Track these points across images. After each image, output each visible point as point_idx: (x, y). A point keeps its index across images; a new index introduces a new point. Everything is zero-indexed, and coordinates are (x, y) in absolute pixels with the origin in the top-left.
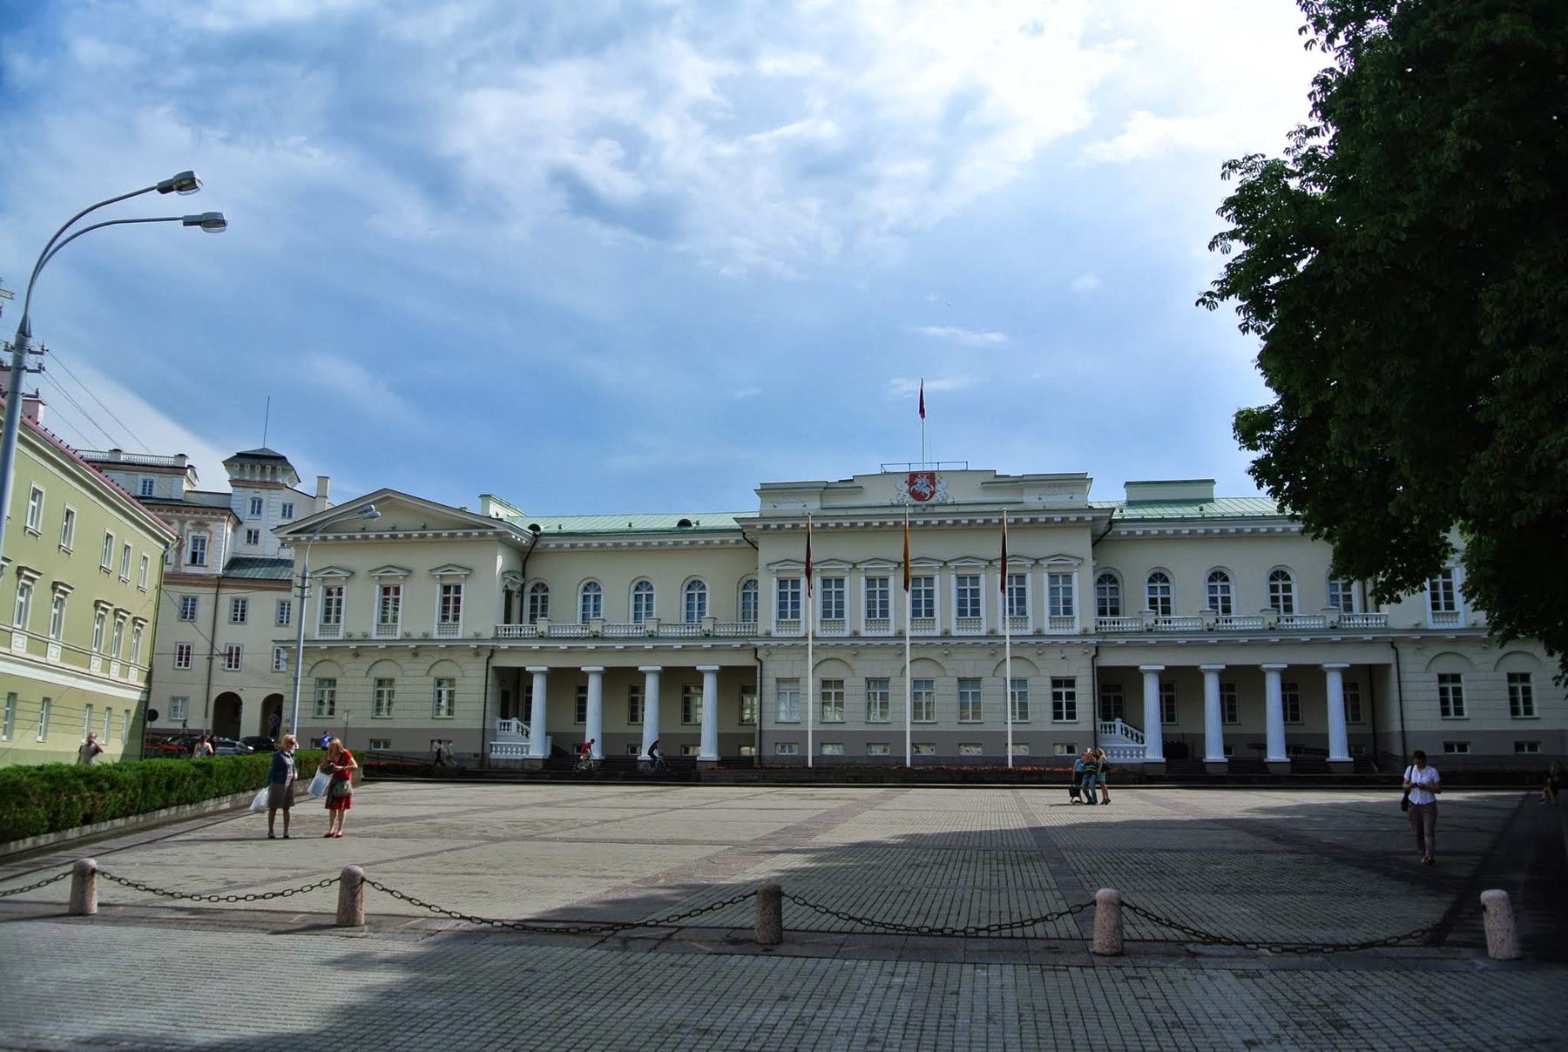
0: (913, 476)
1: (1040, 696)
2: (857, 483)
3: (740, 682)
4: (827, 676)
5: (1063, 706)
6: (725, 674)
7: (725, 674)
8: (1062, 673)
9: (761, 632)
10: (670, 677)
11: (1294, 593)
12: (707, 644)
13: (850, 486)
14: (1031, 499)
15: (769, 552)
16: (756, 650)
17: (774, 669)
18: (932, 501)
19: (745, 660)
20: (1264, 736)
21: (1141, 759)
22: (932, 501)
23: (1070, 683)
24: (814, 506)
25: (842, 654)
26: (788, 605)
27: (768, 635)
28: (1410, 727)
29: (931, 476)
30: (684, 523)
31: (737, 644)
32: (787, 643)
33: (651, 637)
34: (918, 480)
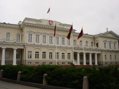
0: (49, 21)
1: (66, 55)
2: (41, 20)
3: (20, 52)
4: (36, 51)
5: (69, 57)
6: (18, 50)
7: (18, 50)
8: (69, 52)
9: (25, 43)
10: (7, 50)
11: (88, 44)
12: (16, 44)
13: (40, 21)
14: (65, 27)
15: (26, 30)
16: (24, 46)
17: (28, 49)
18: (53, 25)
19: (22, 48)
20: (89, 62)
21: (77, 65)
22: (53, 25)
23: (69, 54)
24: (35, 23)
25: (39, 48)
26: (30, 40)
27: (27, 44)
28: (103, 61)
29: (52, 21)
30: (4, 23)
31: (21, 45)
32: (31, 45)
33: (4, 42)
34: (50, 22)
